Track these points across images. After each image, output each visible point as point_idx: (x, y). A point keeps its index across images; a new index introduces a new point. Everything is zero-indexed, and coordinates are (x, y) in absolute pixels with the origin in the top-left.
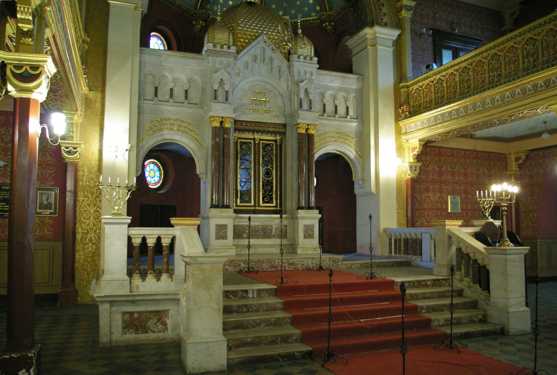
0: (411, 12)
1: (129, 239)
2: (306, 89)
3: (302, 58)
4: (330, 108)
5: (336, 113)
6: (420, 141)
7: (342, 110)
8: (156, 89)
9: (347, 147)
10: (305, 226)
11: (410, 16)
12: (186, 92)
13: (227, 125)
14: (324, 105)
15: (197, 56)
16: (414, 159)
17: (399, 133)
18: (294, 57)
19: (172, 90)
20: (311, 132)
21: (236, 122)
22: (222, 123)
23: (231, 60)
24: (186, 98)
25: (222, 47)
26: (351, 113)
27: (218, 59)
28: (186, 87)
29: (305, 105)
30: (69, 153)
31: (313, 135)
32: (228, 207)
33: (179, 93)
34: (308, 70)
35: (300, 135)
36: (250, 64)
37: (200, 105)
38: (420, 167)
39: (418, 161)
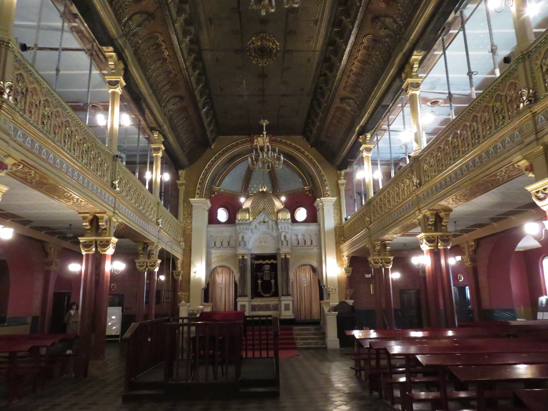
3: (283, 221)
4: (302, 242)
5: (305, 244)
7: (308, 243)
8: (215, 243)
10: (285, 304)
12: (229, 242)
13: (246, 257)
14: (298, 241)
15: (233, 225)
17: (339, 253)
18: (279, 221)
19: (222, 242)
20: (288, 256)
21: (251, 254)
22: (243, 257)
23: (248, 226)
24: (229, 245)
26: (314, 243)
27: (242, 227)
28: (228, 240)
29: (285, 243)
30: (176, 275)
32: (246, 296)
33: (225, 244)
34: (286, 226)
35: (282, 259)
37: (235, 248)
38: (352, 270)
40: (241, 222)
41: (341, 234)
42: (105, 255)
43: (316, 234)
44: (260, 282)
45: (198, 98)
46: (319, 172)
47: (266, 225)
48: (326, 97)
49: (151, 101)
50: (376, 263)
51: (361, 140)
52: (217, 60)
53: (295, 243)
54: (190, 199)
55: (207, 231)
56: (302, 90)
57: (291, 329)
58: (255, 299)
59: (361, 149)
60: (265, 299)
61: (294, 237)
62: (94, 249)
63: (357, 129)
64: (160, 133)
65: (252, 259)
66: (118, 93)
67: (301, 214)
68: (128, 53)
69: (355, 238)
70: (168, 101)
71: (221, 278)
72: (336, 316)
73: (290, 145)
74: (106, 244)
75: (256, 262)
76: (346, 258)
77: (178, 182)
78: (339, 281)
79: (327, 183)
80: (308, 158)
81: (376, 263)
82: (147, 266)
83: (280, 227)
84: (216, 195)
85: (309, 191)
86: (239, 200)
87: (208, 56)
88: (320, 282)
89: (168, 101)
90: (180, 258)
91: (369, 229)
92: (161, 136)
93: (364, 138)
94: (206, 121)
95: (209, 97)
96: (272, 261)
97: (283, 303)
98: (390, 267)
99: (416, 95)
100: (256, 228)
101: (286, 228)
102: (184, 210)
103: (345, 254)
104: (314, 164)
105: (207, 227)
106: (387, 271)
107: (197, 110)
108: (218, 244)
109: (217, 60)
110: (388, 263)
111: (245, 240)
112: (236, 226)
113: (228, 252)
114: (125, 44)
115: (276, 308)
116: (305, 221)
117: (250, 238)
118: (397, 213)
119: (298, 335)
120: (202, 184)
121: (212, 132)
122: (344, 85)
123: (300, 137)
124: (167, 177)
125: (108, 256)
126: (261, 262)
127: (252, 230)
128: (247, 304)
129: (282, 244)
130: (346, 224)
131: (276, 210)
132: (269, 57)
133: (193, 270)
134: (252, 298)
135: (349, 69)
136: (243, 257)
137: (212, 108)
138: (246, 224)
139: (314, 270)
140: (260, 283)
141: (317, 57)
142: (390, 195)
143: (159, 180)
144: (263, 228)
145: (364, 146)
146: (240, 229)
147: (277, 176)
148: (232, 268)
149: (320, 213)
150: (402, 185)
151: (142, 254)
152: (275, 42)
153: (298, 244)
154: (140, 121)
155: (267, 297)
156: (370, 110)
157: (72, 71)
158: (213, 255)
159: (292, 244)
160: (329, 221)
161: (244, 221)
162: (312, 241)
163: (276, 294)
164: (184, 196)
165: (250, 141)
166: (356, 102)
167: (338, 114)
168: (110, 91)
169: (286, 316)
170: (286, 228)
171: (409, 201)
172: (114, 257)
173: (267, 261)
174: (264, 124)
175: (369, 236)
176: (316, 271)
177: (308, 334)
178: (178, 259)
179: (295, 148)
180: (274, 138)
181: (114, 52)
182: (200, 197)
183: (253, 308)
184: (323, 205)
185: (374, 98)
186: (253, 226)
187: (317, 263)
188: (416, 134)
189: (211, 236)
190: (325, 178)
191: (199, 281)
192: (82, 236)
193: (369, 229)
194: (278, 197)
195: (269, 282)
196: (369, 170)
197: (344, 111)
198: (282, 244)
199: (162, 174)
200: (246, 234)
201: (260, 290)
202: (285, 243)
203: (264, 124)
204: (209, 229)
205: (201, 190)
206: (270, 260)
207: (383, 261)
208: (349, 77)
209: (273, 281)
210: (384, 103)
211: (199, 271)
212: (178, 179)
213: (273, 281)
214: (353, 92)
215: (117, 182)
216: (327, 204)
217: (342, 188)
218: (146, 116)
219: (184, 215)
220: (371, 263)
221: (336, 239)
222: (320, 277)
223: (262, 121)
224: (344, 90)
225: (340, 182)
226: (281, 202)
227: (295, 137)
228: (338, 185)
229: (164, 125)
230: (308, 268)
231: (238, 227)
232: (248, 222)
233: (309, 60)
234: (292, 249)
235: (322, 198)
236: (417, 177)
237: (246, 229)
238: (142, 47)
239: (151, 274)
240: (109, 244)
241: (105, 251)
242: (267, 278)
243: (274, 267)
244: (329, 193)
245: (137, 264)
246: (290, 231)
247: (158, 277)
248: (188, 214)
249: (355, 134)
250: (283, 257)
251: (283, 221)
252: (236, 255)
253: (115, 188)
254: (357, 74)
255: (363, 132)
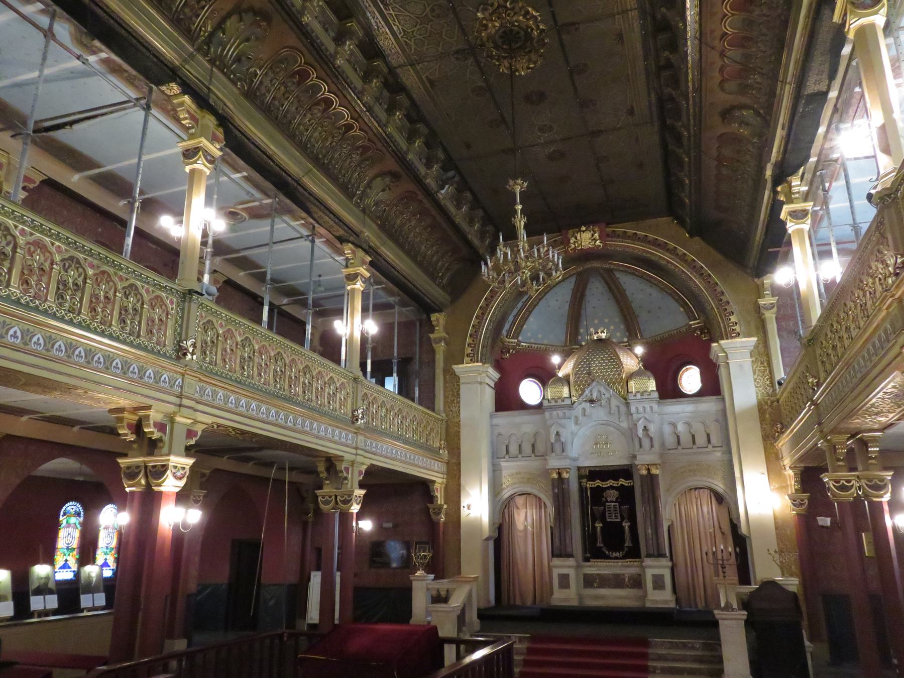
0: (775, 309)
1: (428, 589)
2: (645, 427)
3: (639, 396)
4: (685, 439)
5: (694, 443)
6: (790, 468)
7: (701, 440)
8: (507, 447)
9: (710, 480)
10: (653, 575)
11: (774, 316)
12: (533, 446)
13: (565, 475)
14: (678, 437)
16: (796, 490)
17: (772, 460)
18: (631, 397)
19: (520, 446)
20: (654, 471)
21: (579, 468)
22: (559, 474)
23: (567, 412)
24: (533, 451)
25: (556, 402)
26: (714, 440)
27: (555, 413)
28: (533, 440)
29: (646, 443)
30: (435, 513)
31: (657, 476)
32: (570, 556)
33: (527, 449)
34: (647, 406)
35: (642, 476)
36: (588, 411)
39: (804, 492)
40: (553, 403)
41: (773, 417)
42: (161, 492)
43: (717, 421)
44: (599, 525)
45: (422, 170)
46: (712, 287)
47: (591, 408)
48: (684, 118)
49: (317, 185)
50: (843, 488)
51: (782, 198)
52: (431, 82)
53: (670, 440)
54: (455, 367)
55: (492, 426)
56: (631, 112)
57: (645, 643)
58: (593, 562)
59: (783, 216)
60: (611, 563)
61: (667, 429)
62: (143, 482)
63: (769, 173)
64: (357, 246)
65: (580, 477)
66: (201, 171)
67: (691, 379)
68: (224, 93)
69: (796, 426)
70: (369, 186)
71: (524, 518)
72: (743, 622)
73: (645, 240)
74: (160, 472)
75: (590, 485)
76: (790, 473)
77: (431, 336)
78: (779, 526)
79: (733, 307)
80: (686, 261)
81: (843, 488)
82: (336, 502)
83: (633, 409)
84: (512, 354)
85: (702, 330)
86: (549, 360)
87: (409, 78)
88: (735, 527)
89: (369, 186)
90: (439, 480)
91: (814, 403)
92: (360, 253)
93: (787, 190)
94: (459, 215)
95: (449, 164)
96: (622, 482)
97: (649, 574)
98: (886, 498)
99: (873, 26)
100: (584, 415)
101: (648, 409)
102: (445, 387)
103: (787, 462)
104: (700, 273)
105: (491, 416)
106: (877, 509)
107: (430, 195)
108: (514, 449)
109: (431, 82)
110: (878, 488)
111: (563, 439)
112: (543, 413)
113: (532, 464)
114: (211, 74)
115: (637, 582)
116: (699, 394)
117: (573, 434)
118: (863, 358)
119: (660, 658)
120: (474, 336)
121: (482, 235)
122: (717, 77)
123: (664, 220)
124: (372, 327)
125: (168, 495)
126: (598, 483)
127: (576, 417)
128: (572, 573)
129: (641, 446)
130: (783, 392)
131: (624, 375)
132: (530, 52)
133: (464, 502)
134: (587, 560)
135: (718, 34)
136: (559, 474)
137: (463, 186)
138: (563, 407)
139: (719, 499)
140: (599, 529)
141: (637, 26)
142: (847, 314)
143: (357, 336)
144: (599, 414)
145: (786, 209)
146: (551, 417)
147: (633, 305)
148: (542, 496)
149: (722, 372)
150: (870, 280)
151: (327, 479)
152: (528, 12)
153: (679, 443)
154: (314, 227)
155: (616, 558)
156: (783, 117)
157: (159, 151)
158: (505, 473)
159: (663, 444)
160: (745, 390)
161: (560, 402)
162: (708, 435)
163: (634, 553)
164: (444, 362)
165: (562, 243)
166: (758, 114)
167: (727, 152)
168: (187, 169)
169: (657, 601)
170: (648, 409)
171: (883, 320)
172: (182, 497)
173: (611, 483)
174: (518, 189)
175: (818, 419)
176: (724, 500)
177: (683, 659)
178: (434, 482)
179: (655, 243)
180: (609, 230)
181: (184, 92)
182: (472, 361)
183: (589, 581)
184: (727, 357)
185: (784, 82)
186: (578, 410)
187: (726, 485)
188: (883, 129)
189: (500, 434)
190: (727, 297)
191: (476, 525)
192: (125, 455)
193: (814, 403)
194: (630, 348)
195: (619, 525)
196: (805, 262)
197: (736, 139)
198: (641, 446)
199: (362, 323)
200: (564, 427)
201: (600, 544)
202: (646, 443)
203: (518, 189)
204: (496, 421)
205: (474, 346)
206: (617, 480)
207: (863, 482)
208: (722, 54)
209: (626, 525)
210: (812, 87)
211: (476, 505)
212: (433, 332)
213: (626, 525)
214: (744, 89)
215: (189, 343)
216: (737, 353)
217: (770, 316)
218: (316, 216)
219: (446, 397)
220: (829, 489)
221: (763, 429)
222: (734, 517)
223: (511, 182)
224: (722, 89)
225: (761, 302)
226: (636, 356)
227: (652, 222)
228: (758, 309)
229: (364, 230)
230: (705, 494)
231: (547, 414)
232: (568, 402)
233: (620, 37)
234: (661, 455)
235: (722, 342)
236: (896, 249)
237: (564, 417)
238: (267, 82)
239: (345, 517)
240: (166, 470)
241: (160, 485)
242: (612, 518)
243: (626, 495)
244: (737, 328)
245: (320, 498)
246: (656, 417)
247: (357, 524)
248: (453, 395)
249: (769, 185)
250: (644, 472)
251: (639, 396)
252: (547, 472)
253: (185, 354)
254: (742, 42)
255: (782, 175)
